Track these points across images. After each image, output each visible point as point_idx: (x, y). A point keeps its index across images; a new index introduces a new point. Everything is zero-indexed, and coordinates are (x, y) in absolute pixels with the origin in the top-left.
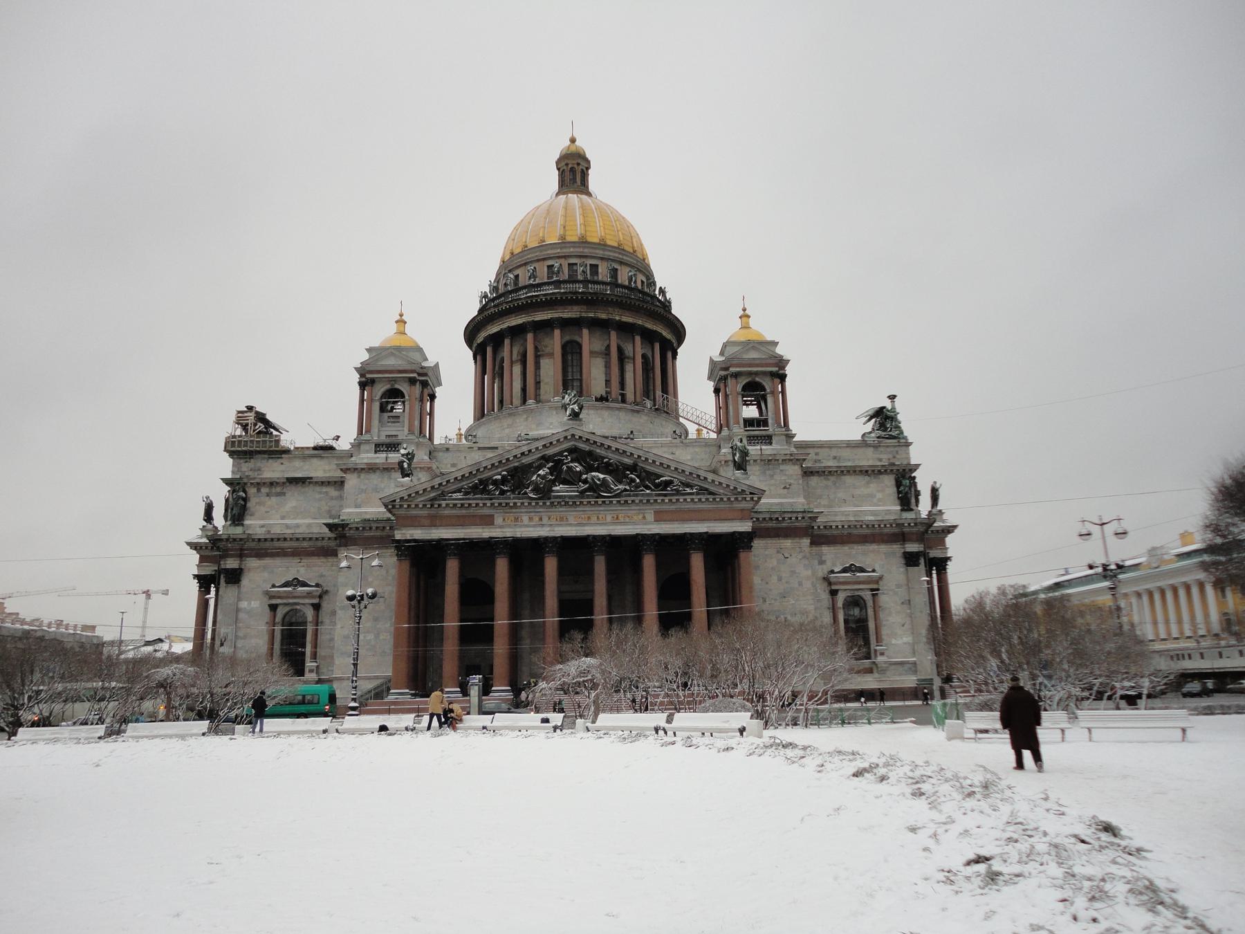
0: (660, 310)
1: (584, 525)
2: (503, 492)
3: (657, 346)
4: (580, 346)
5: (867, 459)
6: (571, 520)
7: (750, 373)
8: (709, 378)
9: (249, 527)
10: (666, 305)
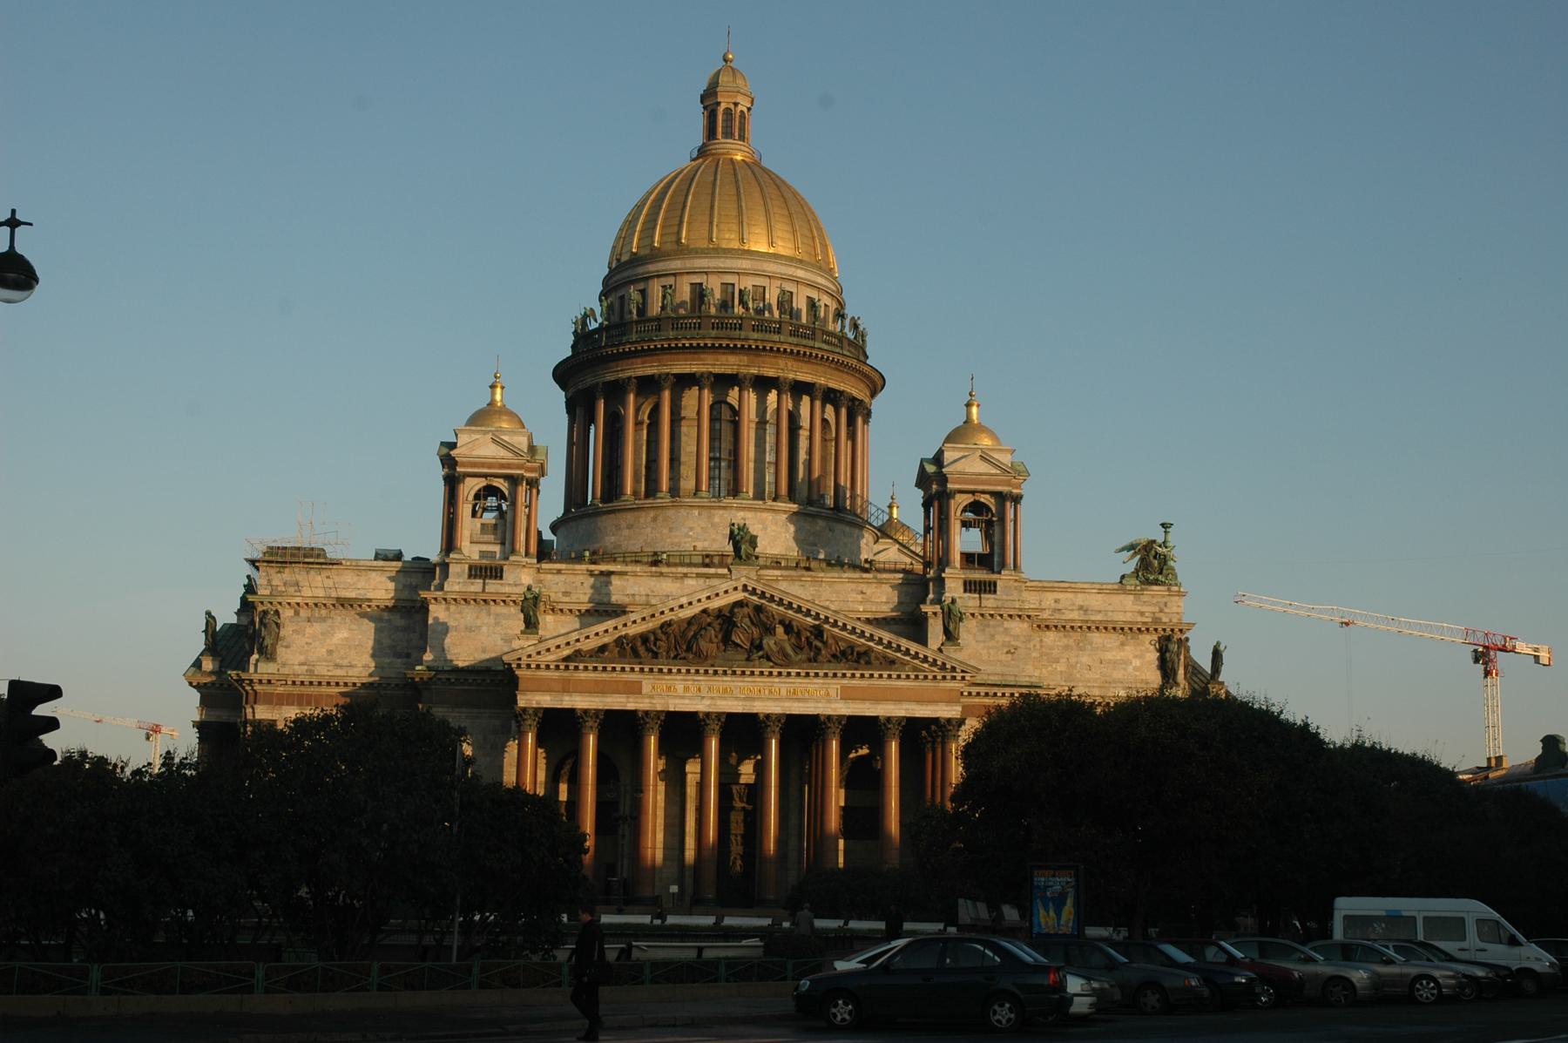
0: (850, 349)
1: (753, 699)
2: (655, 655)
3: (843, 411)
4: (736, 412)
5: (1126, 608)
6: (736, 693)
7: (973, 492)
8: (918, 485)
9: (284, 665)
10: (858, 347)
